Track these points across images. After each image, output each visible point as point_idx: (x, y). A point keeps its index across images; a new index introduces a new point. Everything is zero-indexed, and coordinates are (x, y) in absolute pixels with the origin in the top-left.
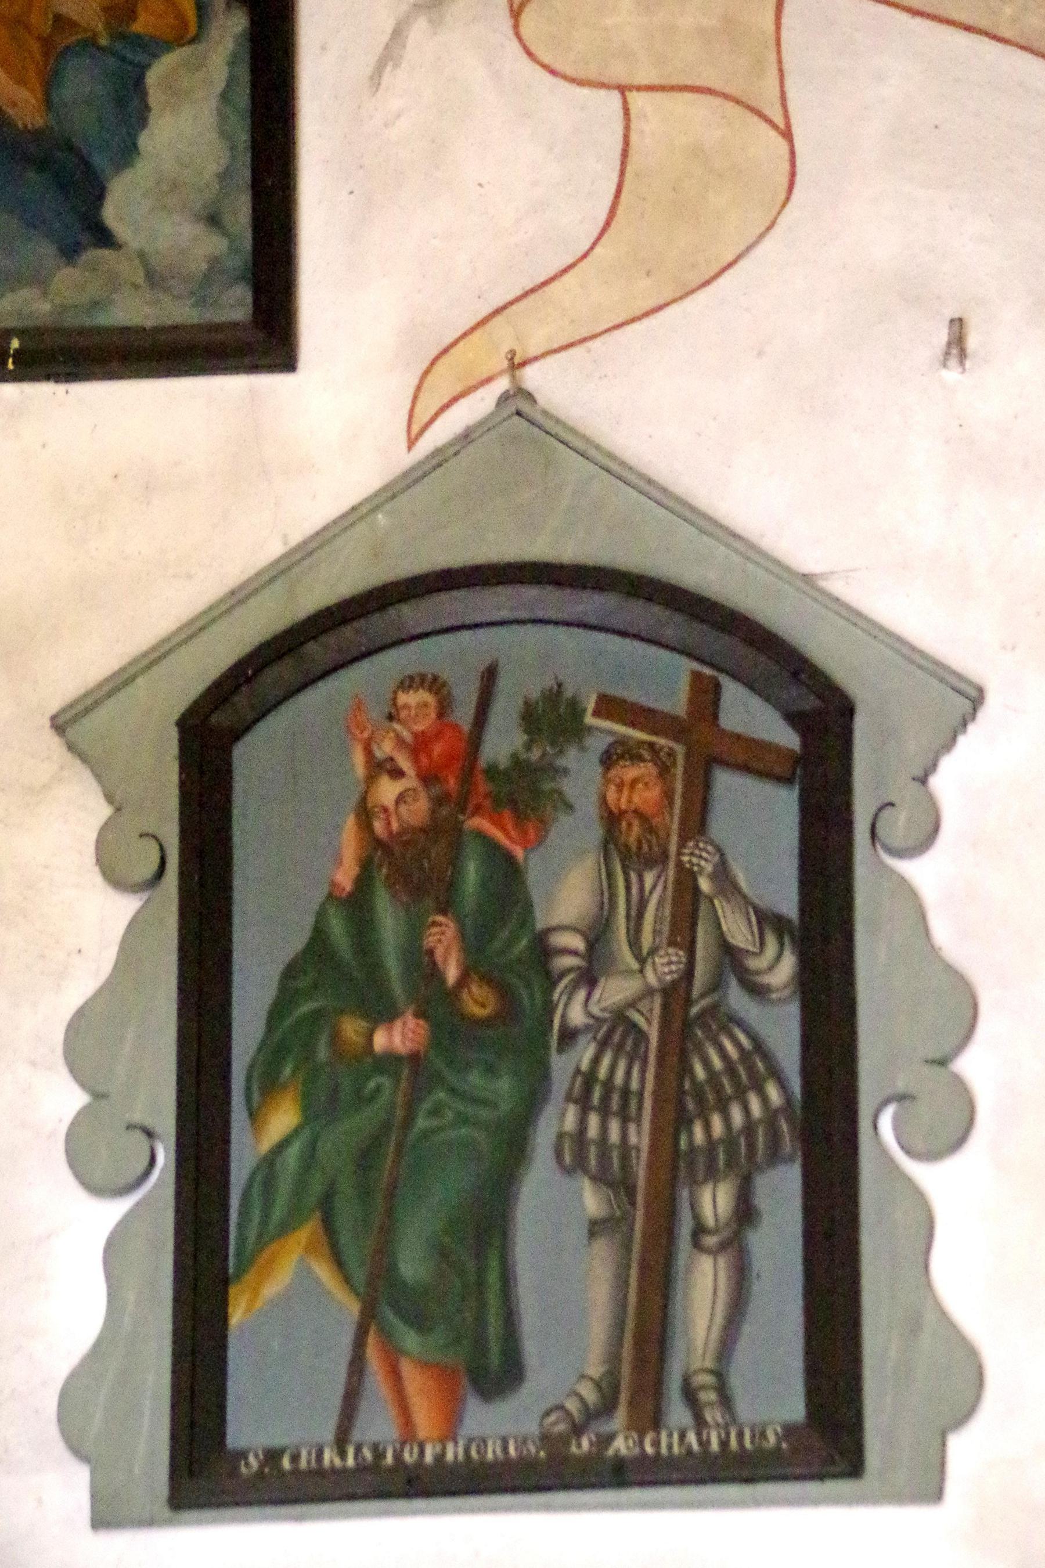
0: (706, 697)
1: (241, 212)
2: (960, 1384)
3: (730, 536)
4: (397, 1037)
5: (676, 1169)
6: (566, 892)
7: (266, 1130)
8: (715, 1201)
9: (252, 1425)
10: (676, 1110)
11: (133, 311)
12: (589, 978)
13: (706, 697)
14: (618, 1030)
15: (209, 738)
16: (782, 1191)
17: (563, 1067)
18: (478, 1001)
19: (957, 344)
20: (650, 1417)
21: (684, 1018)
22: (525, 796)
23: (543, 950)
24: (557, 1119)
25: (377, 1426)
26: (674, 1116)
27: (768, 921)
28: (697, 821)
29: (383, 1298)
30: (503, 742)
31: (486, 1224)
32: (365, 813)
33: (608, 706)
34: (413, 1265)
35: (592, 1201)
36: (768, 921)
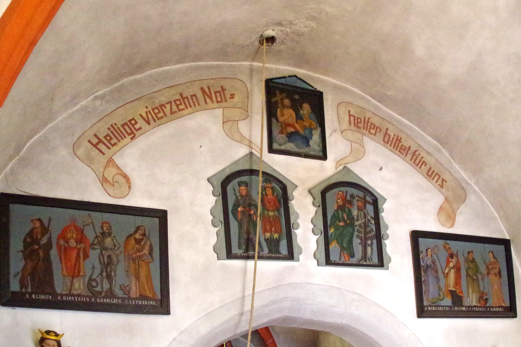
0: (365, 197)
1: (321, 146)
2: (390, 260)
3: (365, 182)
4: (341, 224)
5: (366, 239)
6: (355, 213)
7: (331, 231)
8: (369, 242)
9: (333, 258)
10: (366, 233)
11: (312, 153)
12: (357, 220)
13: (365, 197)
14: (360, 226)
15: (324, 193)
16: (375, 242)
17: (356, 228)
18: (348, 221)
19: (381, 169)
20: (366, 261)
21: (366, 226)
22: (350, 203)
23: (354, 218)
24: (356, 233)
25: (343, 259)
26: (365, 234)
27: (372, 217)
28: (365, 208)
29: (342, 248)
30: (348, 198)
31: (350, 242)
32: (337, 203)
33: (357, 196)
34: (345, 245)
35: (359, 241)
36: (372, 217)
